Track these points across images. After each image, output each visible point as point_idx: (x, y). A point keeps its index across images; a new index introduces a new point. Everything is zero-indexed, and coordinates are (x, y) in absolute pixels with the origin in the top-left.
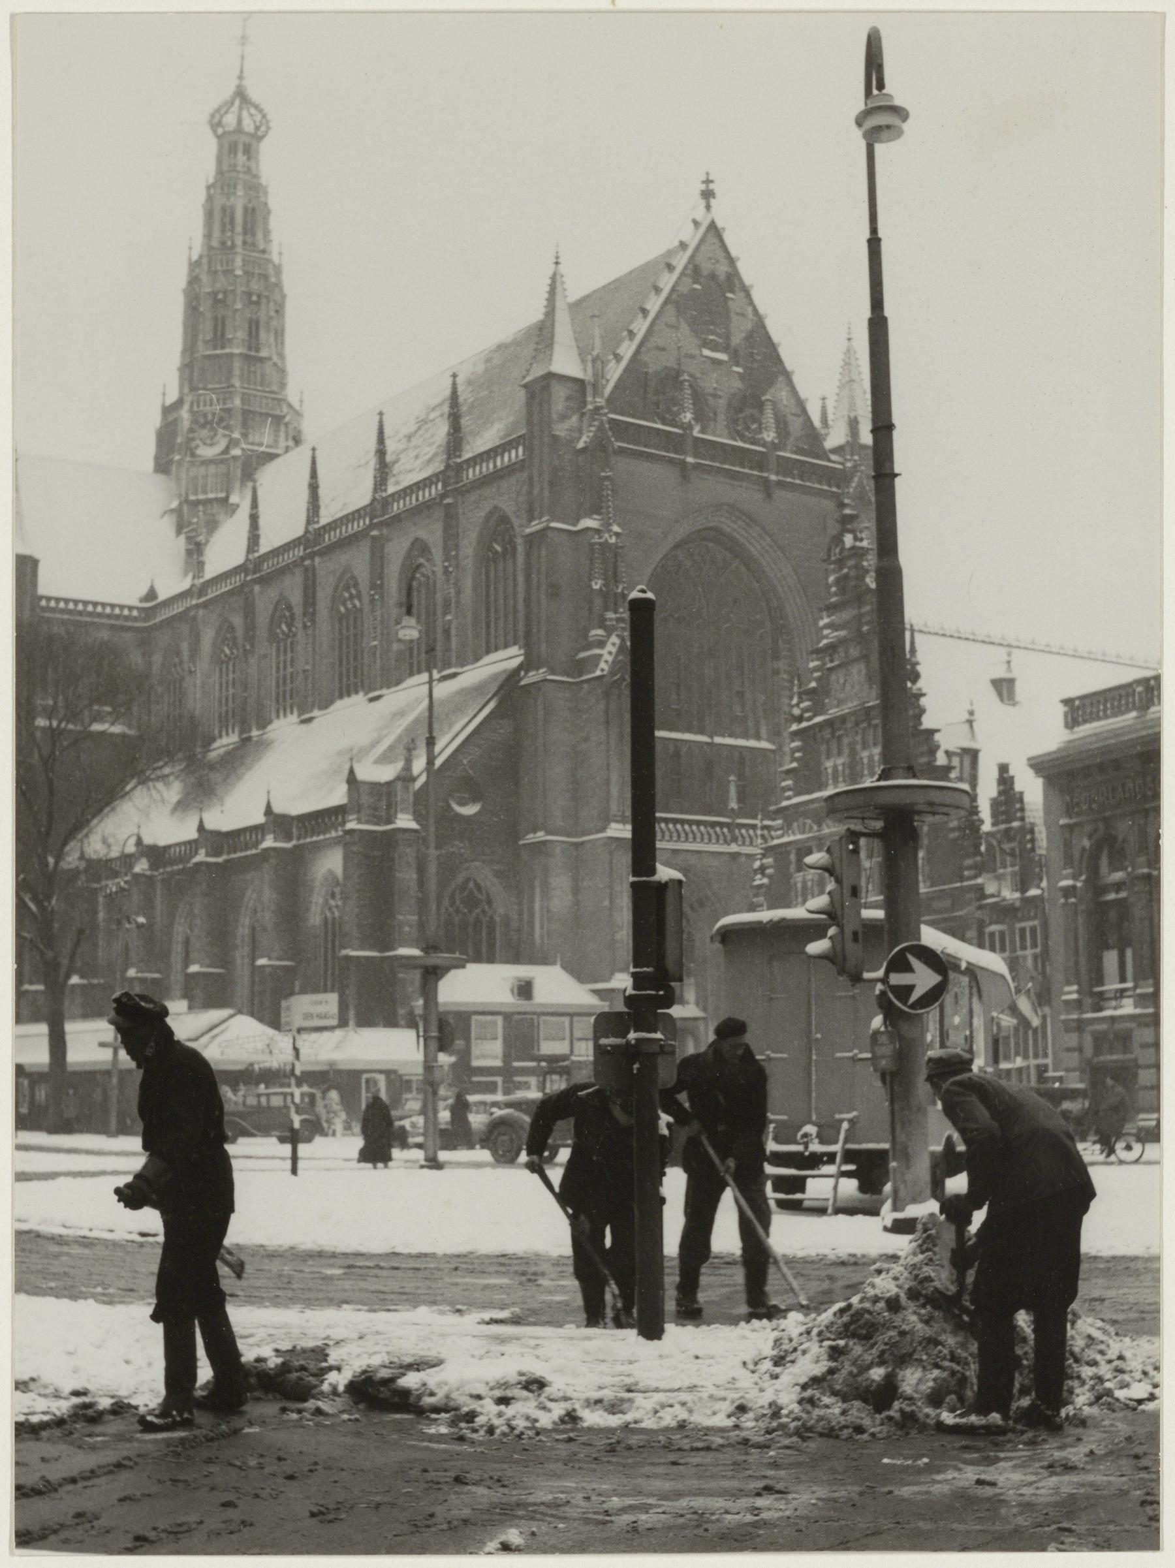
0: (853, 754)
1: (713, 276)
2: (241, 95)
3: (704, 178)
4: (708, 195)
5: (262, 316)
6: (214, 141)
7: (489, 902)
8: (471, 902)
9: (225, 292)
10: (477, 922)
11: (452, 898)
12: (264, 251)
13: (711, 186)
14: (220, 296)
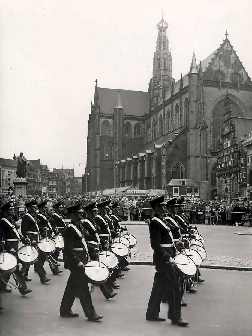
0: (227, 142)
1: (227, 51)
2: (163, 20)
3: (226, 32)
4: (227, 35)
5: (167, 62)
6: (158, 30)
7: (181, 167)
8: (178, 167)
9: (160, 58)
10: (179, 171)
11: (174, 167)
12: (167, 50)
13: (228, 33)
14: (159, 59)
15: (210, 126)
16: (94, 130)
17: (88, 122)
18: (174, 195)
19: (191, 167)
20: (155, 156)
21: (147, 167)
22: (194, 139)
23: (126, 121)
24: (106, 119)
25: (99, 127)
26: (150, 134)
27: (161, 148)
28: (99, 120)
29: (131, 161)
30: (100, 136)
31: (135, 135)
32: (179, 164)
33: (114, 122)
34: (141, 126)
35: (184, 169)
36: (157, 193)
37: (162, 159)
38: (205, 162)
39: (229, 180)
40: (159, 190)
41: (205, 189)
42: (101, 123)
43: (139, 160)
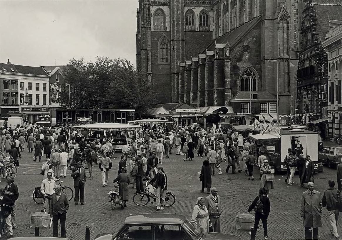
7: (254, 74)
15: (295, 14)
16: (143, 23)
17: (138, 11)
19: (266, 74)
22: (271, 34)
23: (186, 9)
24: (160, 7)
25: (150, 18)
26: (221, 25)
28: (149, 9)
30: (152, 30)
32: (249, 70)
33: (170, 10)
34: (208, 15)
35: (257, 77)
37: (226, 64)
39: (309, 94)
42: (152, 13)
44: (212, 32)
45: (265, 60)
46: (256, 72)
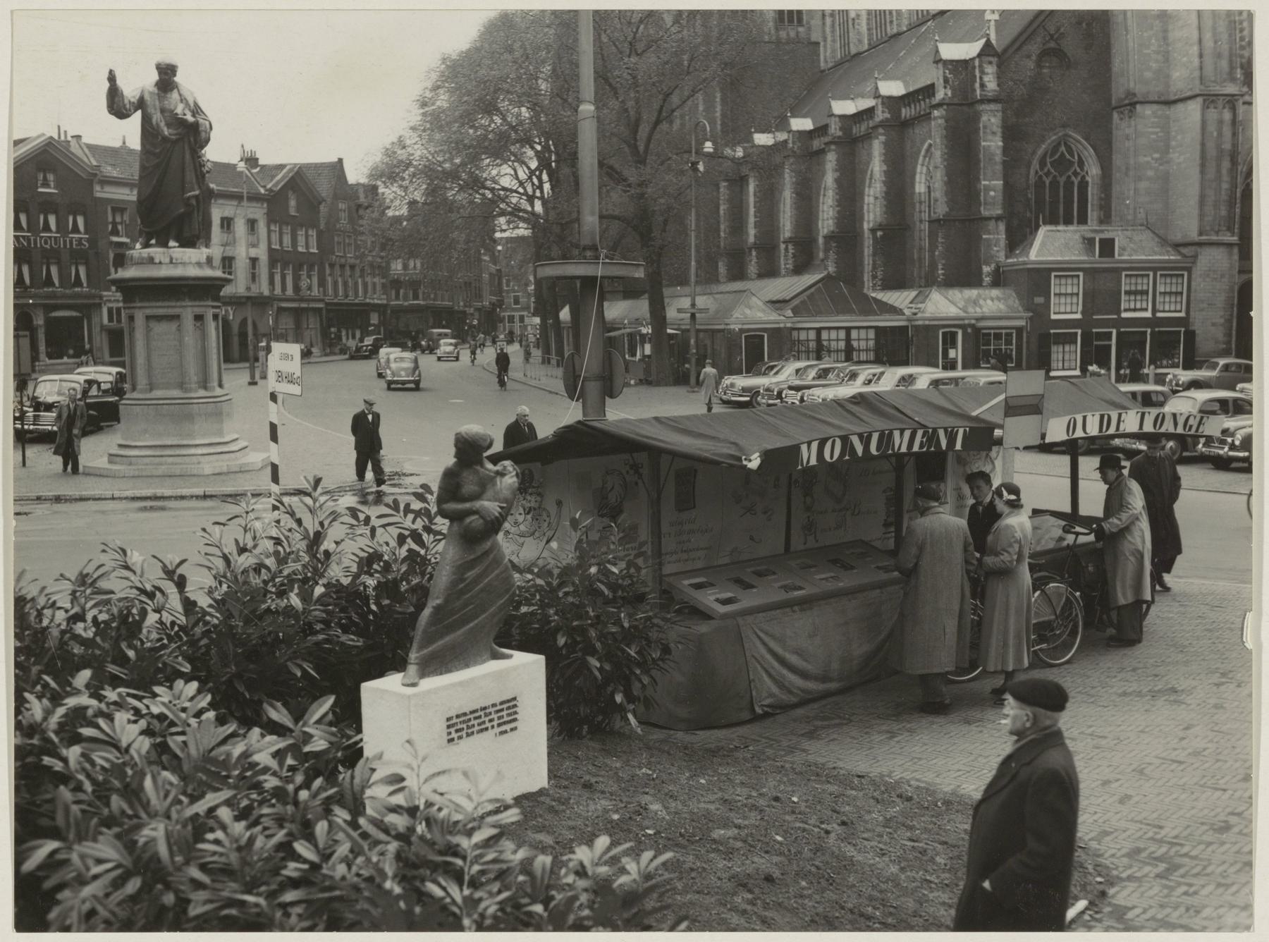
7: (1081, 163)
10: (1069, 184)
11: (1042, 163)
18: (1053, 317)
20: (939, 105)
21: (885, 168)
27: (973, 59)
29: (779, 147)
31: (777, 29)
32: (1065, 143)
35: (1093, 171)
36: (961, 304)
38: (1227, 131)
40: (973, 293)
41: (1222, 276)
43: (827, 139)
44: (818, 44)
45: (1133, 105)
46: (1089, 155)
